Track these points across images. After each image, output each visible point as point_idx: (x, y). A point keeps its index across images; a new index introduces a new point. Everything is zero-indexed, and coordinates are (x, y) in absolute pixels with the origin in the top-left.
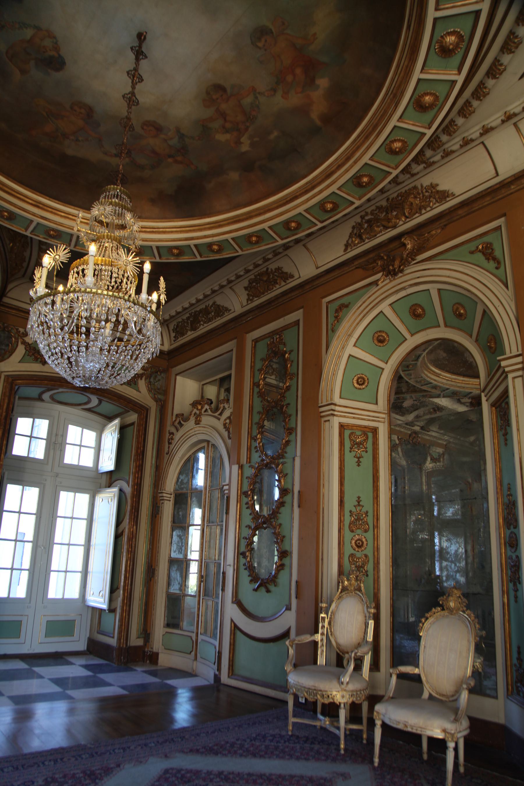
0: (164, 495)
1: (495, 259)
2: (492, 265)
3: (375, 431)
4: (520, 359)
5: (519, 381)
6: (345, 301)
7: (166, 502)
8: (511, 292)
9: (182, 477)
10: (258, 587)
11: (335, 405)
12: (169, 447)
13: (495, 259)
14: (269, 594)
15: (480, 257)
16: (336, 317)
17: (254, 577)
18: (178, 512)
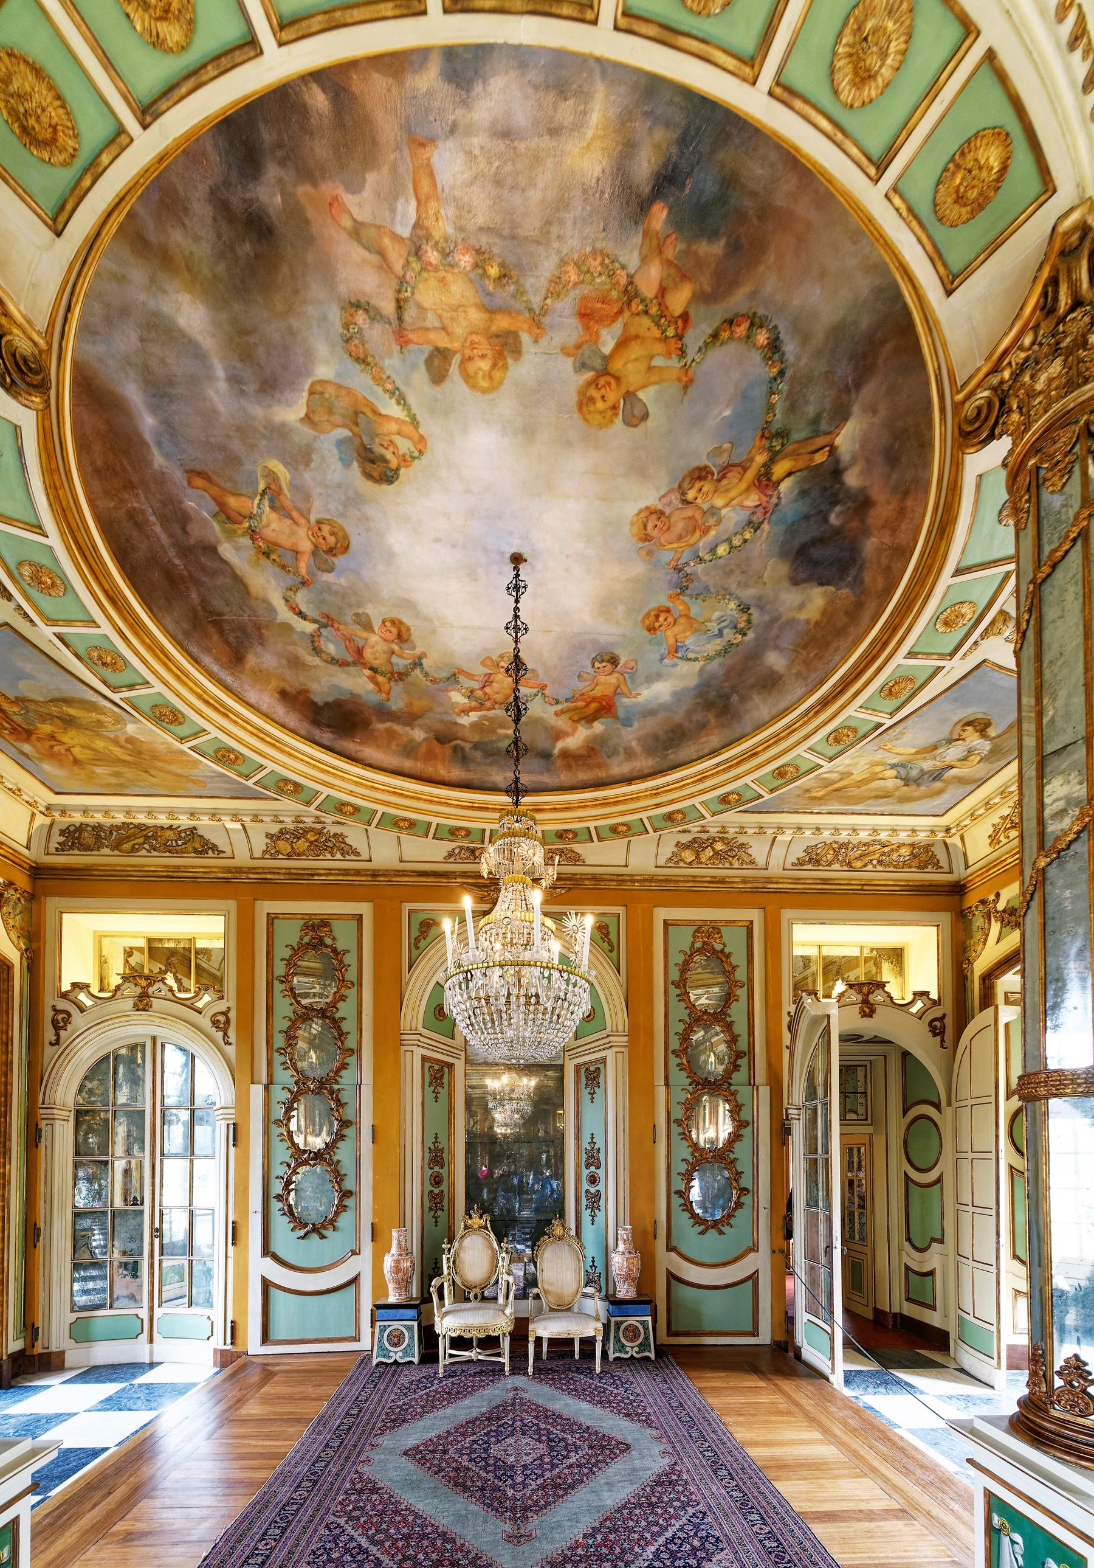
0: (55, 1111)
2: (606, 945)
4: (626, 1039)
5: (620, 1056)
7: (58, 1122)
9: (89, 1085)
10: (306, 1234)
11: (420, 1034)
12: (58, 1035)
14: (324, 1241)
16: (422, 932)
17: (298, 1222)
18: (86, 1139)
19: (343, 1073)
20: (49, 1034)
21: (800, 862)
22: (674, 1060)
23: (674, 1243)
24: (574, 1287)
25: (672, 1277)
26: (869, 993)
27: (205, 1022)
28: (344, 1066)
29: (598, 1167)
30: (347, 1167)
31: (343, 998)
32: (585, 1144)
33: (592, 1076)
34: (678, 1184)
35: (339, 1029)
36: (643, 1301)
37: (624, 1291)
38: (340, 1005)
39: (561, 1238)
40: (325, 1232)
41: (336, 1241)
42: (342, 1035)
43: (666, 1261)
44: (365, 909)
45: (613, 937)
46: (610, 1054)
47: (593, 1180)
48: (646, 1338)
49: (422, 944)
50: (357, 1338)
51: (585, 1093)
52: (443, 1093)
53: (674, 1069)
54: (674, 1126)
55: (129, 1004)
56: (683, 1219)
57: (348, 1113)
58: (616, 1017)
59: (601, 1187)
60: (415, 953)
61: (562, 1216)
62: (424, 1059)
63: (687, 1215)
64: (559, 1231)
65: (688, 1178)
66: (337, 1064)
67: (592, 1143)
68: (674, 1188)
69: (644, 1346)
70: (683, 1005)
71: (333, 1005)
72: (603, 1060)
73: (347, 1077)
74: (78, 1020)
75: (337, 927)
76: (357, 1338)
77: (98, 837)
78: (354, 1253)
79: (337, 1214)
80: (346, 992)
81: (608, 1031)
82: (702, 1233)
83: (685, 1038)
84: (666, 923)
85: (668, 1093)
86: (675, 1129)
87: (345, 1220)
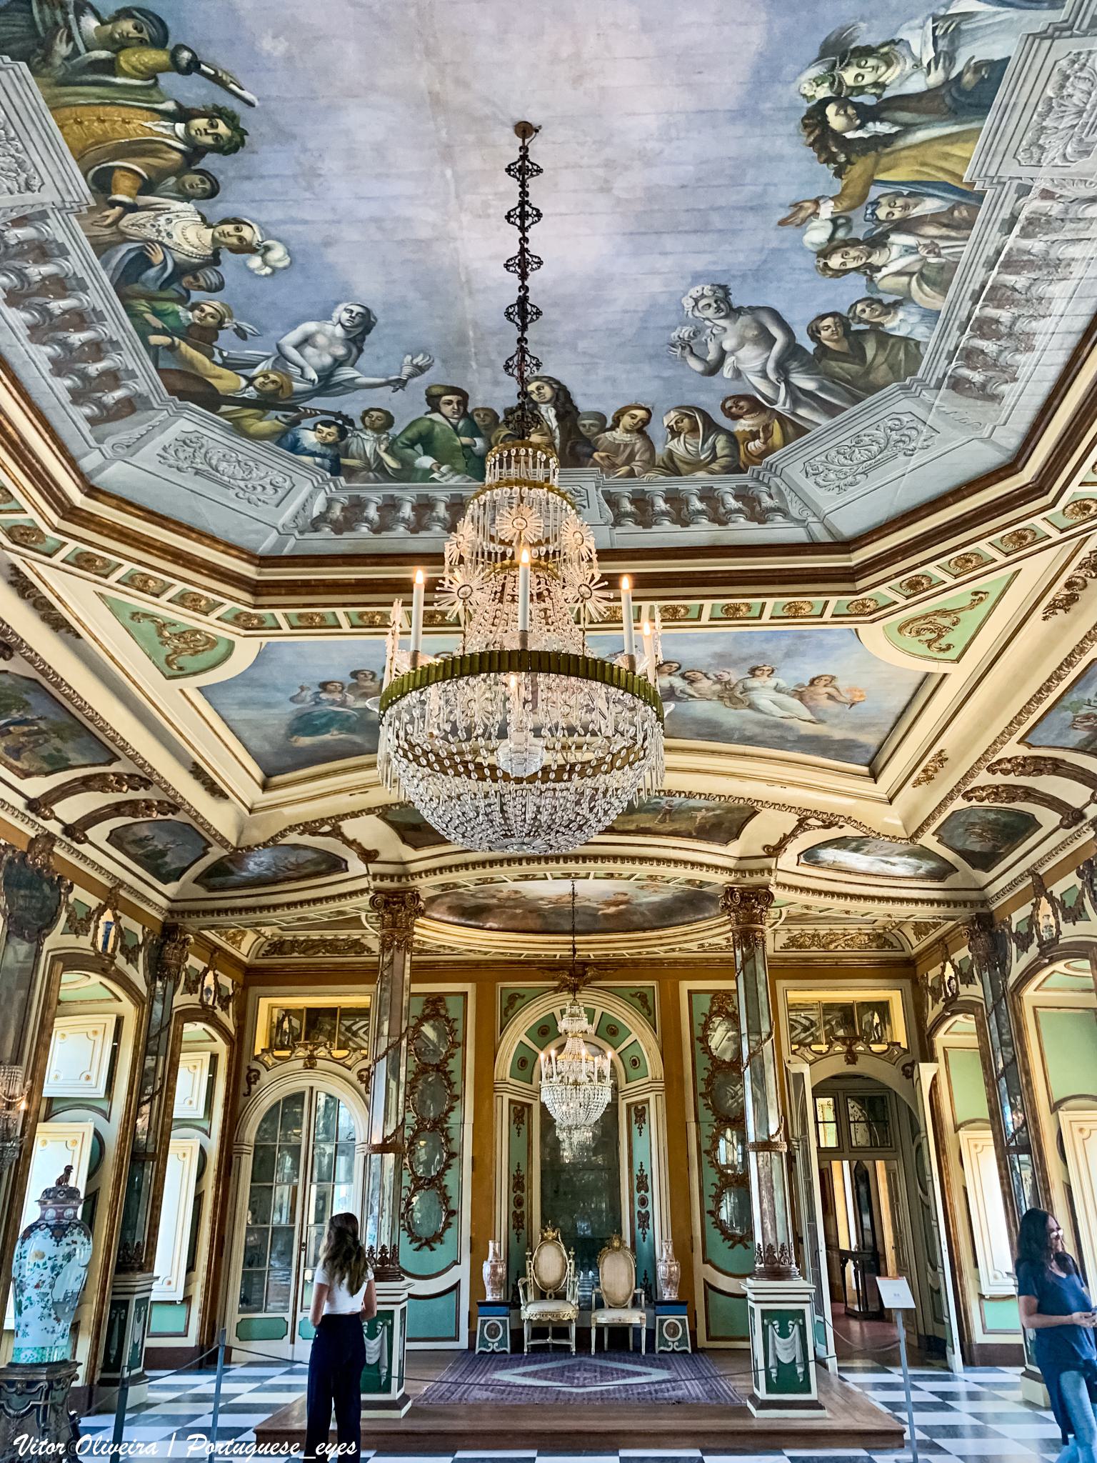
1: (648, 1009)
2: (645, 1011)
3: (530, 1106)
6: (522, 992)
8: (658, 1036)
13: (648, 1009)
15: (637, 1001)
17: (414, 1238)
19: (451, 1114)
20: (243, 1088)
21: (786, 946)
22: (701, 1101)
23: (709, 1257)
24: (627, 1290)
25: (709, 1287)
26: (850, 1046)
27: (353, 1076)
28: (451, 1109)
29: (647, 1191)
30: (452, 1192)
31: (452, 1056)
32: (636, 1172)
33: (639, 1113)
34: (710, 1205)
35: (448, 1080)
36: (683, 1304)
37: (668, 1294)
38: (450, 1061)
39: (618, 1249)
40: (434, 1245)
41: (442, 1254)
42: (451, 1084)
43: (704, 1272)
44: (469, 987)
45: (650, 1004)
46: (651, 1096)
47: (643, 1202)
48: (684, 1334)
49: (510, 1013)
50: (456, 1339)
51: (635, 1127)
52: (524, 1128)
53: (701, 1108)
54: (704, 1155)
55: (300, 1064)
56: (715, 1235)
57: (454, 1147)
58: (654, 1065)
59: (649, 1208)
60: (505, 1019)
61: (620, 1232)
62: (511, 1101)
63: (718, 1231)
64: (616, 1244)
65: (718, 1199)
66: (446, 1107)
67: (642, 1170)
68: (707, 1208)
69: (682, 1341)
70: (707, 1056)
71: (445, 1061)
72: (647, 1101)
73: (454, 1118)
74: (265, 1077)
75: (450, 1002)
76: (456, 1339)
77: (293, 946)
78: (456, 1263)
79: (444, 1229)
80: (455, 1051)
81: (649, 1078)
82: (731, 1247)
83: (709, 1082)
84: (690, 992)
85: (698, 1129)
86: (705, 1158)
87: (449, 1234)
